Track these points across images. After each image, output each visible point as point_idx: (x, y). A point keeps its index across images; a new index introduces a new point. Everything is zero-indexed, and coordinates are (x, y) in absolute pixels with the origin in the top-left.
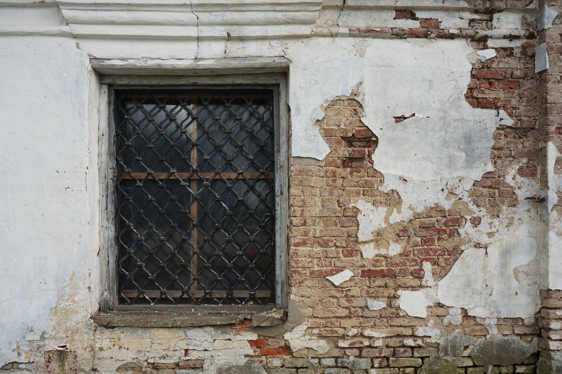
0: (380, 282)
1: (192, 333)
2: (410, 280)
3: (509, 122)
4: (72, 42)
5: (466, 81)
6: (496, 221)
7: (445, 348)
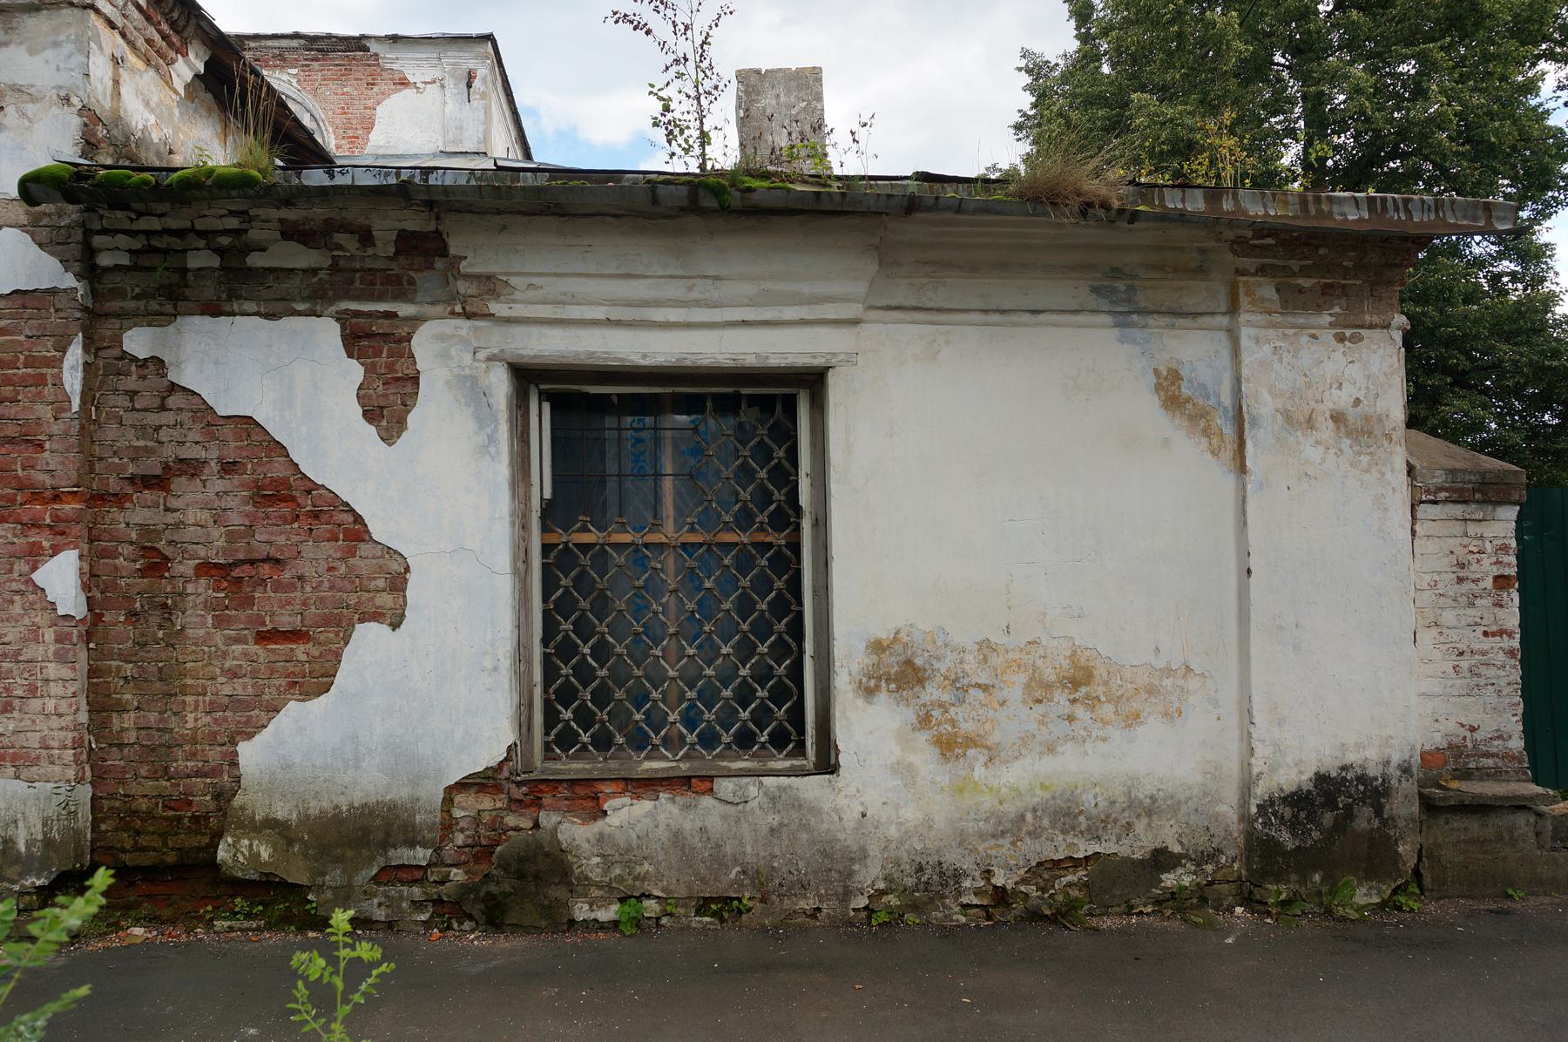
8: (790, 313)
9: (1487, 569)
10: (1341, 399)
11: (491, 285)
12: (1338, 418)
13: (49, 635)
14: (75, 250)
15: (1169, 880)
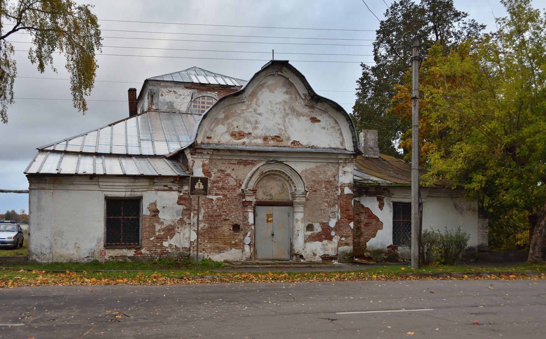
0: (159, 240)
2: (165, 239)
5: (177, 200)
6: (182, 228)
7: (172, 253)
11: (393, 194)
13: (350, 231)
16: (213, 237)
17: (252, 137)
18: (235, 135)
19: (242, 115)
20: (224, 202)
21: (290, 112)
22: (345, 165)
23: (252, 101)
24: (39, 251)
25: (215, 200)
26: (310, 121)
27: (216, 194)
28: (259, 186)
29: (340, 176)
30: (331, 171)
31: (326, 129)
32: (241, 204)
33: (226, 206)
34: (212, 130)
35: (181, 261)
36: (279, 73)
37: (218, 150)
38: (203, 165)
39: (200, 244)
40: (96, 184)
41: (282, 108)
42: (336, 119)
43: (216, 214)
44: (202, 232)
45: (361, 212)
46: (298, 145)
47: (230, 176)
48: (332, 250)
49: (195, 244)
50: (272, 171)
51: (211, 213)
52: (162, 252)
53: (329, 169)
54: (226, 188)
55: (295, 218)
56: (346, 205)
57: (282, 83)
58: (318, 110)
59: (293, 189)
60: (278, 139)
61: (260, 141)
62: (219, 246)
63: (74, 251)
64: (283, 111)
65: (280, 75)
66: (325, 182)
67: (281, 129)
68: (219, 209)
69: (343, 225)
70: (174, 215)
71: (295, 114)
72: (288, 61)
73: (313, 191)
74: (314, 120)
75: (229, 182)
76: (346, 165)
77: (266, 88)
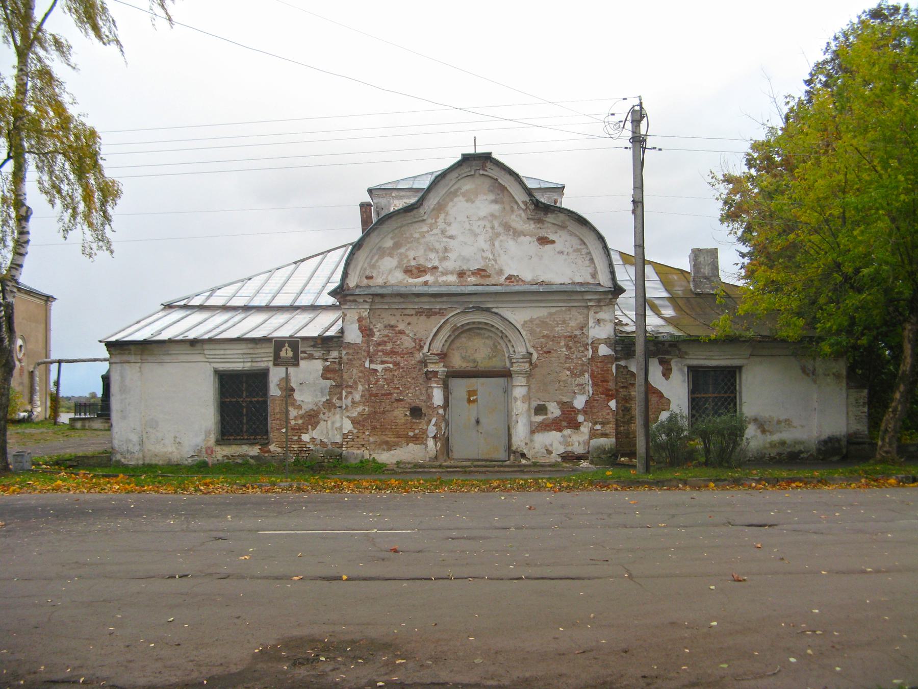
0: (296, 431)
1: (243, 446)
2: (305, 431)
3: (334, 384)
4: (208, 364)
5: (321, 372)
8: (737, 357)
9: (861, 401)
10: (834, 370)
11: (686, 353)
12: (834, 374)
13: (611, 414)
14: (613, 348)
15: (802, 456)
16: (378, 427)
17: (438, 274)
18: (411, 271)
19: (422, 241)
20: (396, 373)
21: (503, 231)
22: (598, 310)
23: (438, 217)
24: (125, 448)
25: (380, 371)
26: (536, 243)
27: (383, 362)
28: (454, 346)
29: (591, 327)
30: (576, 320)
31: (565, 253)
32: (424, 376)
33: (399, 380)
34: (373, 265)
35: (329, 462)
36: (481, 172)
37: (382, 296)
38: (360, 320)
39: (358, 437)
40: (200, 353)
41: (488, 225)
42: (581, 237)
43: (383, 392)
44: (361, 419)
45: (630, 384)
46: (518, 281)
47: (405, 333)
48: (579, 444)
49: (349, 437)
50: (474, 323)
51: (374, 391)
52: (300, 449)
53: (571, 316)
54: (398, 352)
55: (513, 396)
56: (603, 372)
57: (488, 186)
58: (550, 225)
59: (511, 350)
60: (483, 273)
61: (452, 278)
62: (388, 439)
63: (174, 448)
64: (490, 230)
65: (483, 175)
66: (566, 337)
67: (486, 258)
68: (388, 384)
69: (598, 404)
70: (317, 395)
71: (511, 233)
72: (490, 153)
73: (545, 352)
74: (544, 241)
75: (402, 343)
76: (601, 309)
77: (461, 197)
